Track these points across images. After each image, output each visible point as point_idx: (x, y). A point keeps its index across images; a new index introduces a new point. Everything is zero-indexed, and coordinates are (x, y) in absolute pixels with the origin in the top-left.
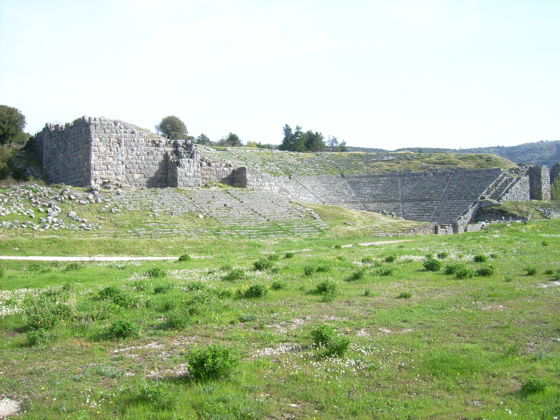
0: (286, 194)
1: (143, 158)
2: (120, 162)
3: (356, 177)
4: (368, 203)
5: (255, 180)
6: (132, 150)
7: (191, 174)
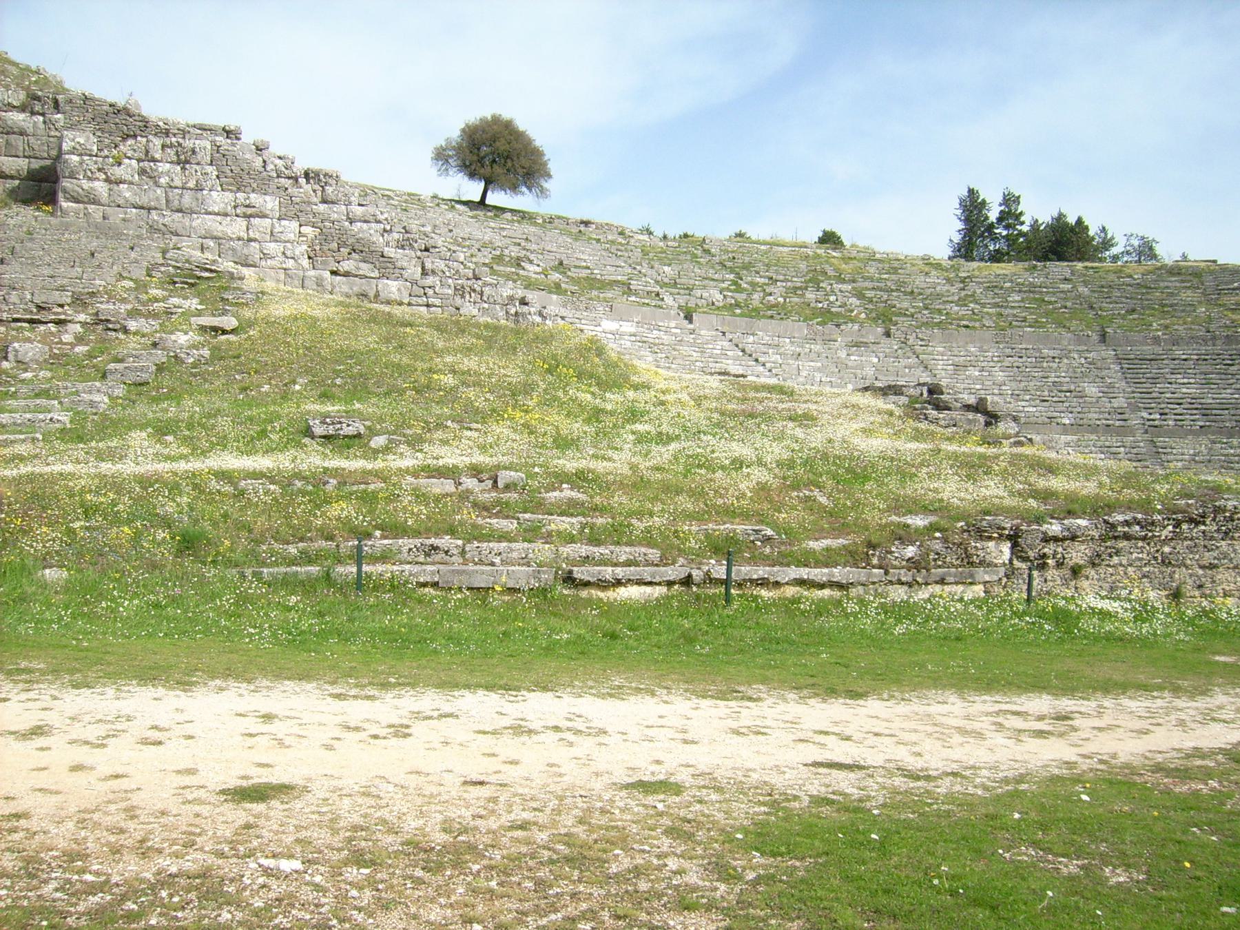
0: (365, 269)
3: (1156, 340)
4: (1171, 434)
5: (128, 170)
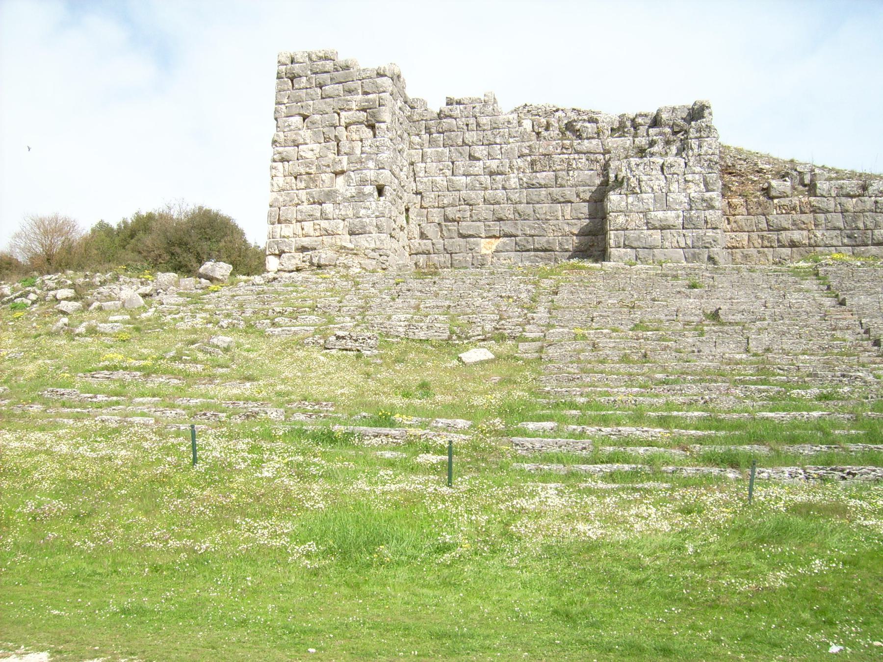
1: (513, 182)
2: (369, 189)
6: (472, 157)
7: (671, 215)
